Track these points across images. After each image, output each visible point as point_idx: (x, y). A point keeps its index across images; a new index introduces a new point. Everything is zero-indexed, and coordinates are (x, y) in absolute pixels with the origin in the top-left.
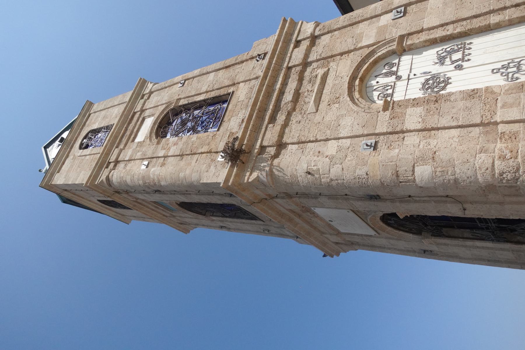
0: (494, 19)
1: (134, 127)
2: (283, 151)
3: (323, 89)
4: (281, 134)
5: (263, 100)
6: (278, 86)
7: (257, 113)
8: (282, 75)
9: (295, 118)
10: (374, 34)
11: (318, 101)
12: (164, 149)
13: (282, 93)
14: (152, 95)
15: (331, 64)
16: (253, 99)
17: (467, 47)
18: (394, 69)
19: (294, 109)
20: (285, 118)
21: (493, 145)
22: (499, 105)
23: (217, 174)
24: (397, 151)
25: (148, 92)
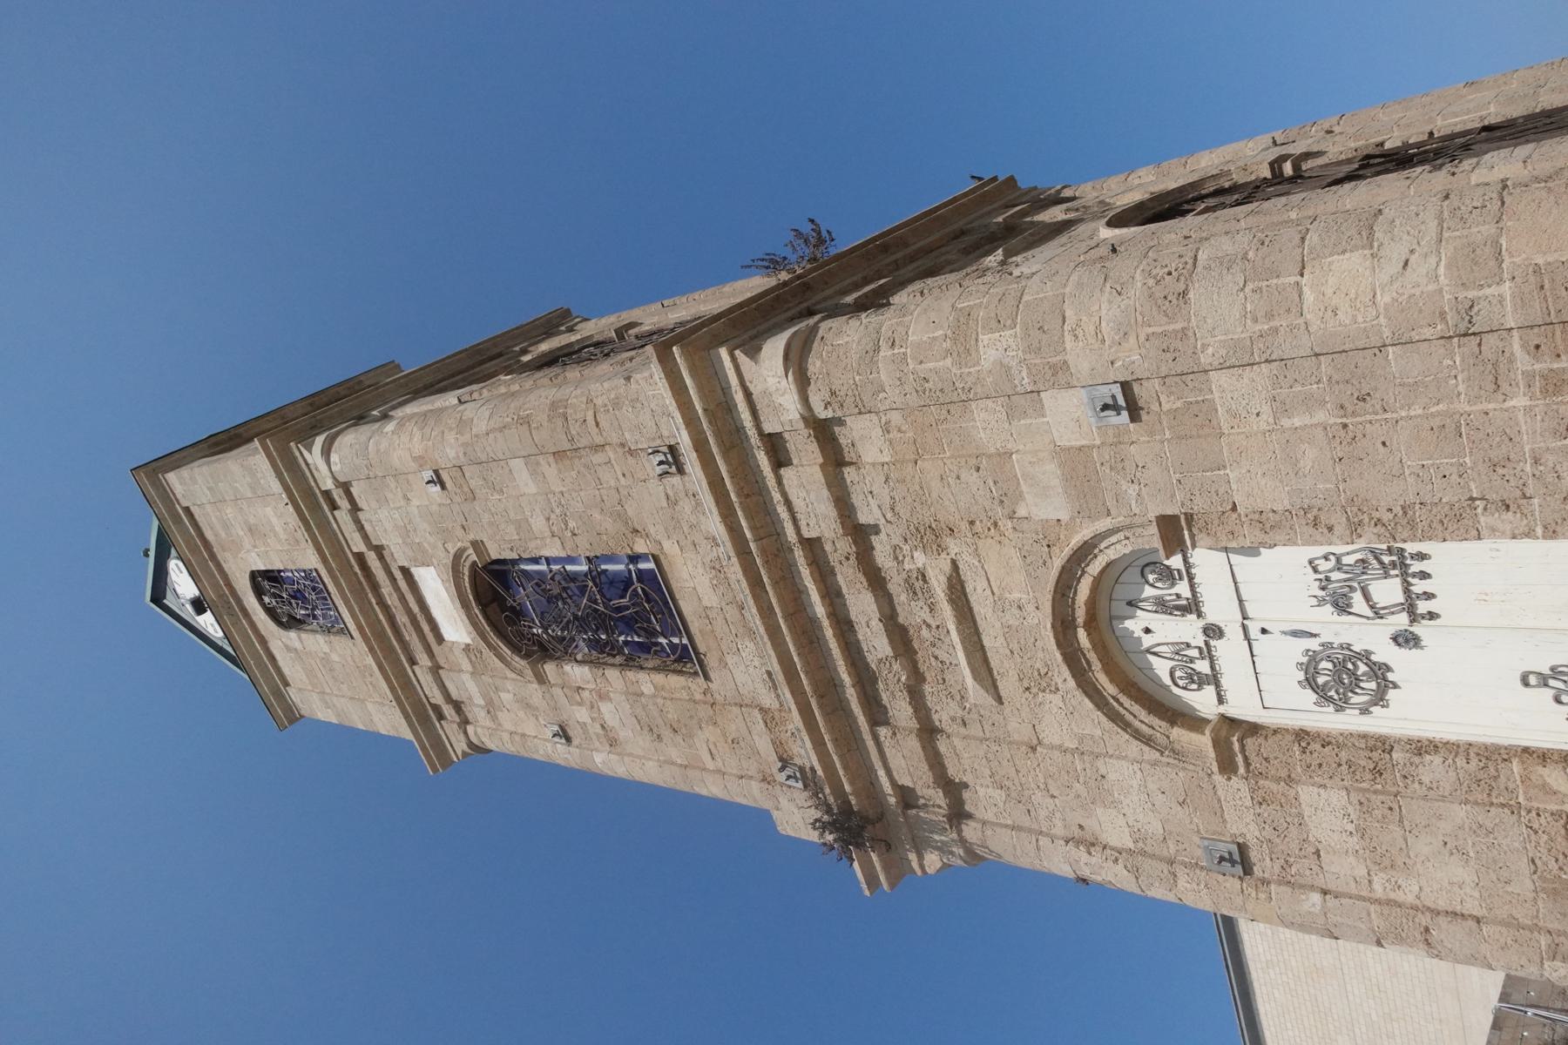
1: (402, 598)
3: (978, 633)
5: (806, 663)
6: (820, 610)
7: (821, 707)
8: (805, 572)
10: (1056, 482)
11: (983, 671)
13: (844, 626)
15: (954, 546)
16: (751, 602)
17: (1416, 567)
18: (1183, 588)
20: (910, 710)
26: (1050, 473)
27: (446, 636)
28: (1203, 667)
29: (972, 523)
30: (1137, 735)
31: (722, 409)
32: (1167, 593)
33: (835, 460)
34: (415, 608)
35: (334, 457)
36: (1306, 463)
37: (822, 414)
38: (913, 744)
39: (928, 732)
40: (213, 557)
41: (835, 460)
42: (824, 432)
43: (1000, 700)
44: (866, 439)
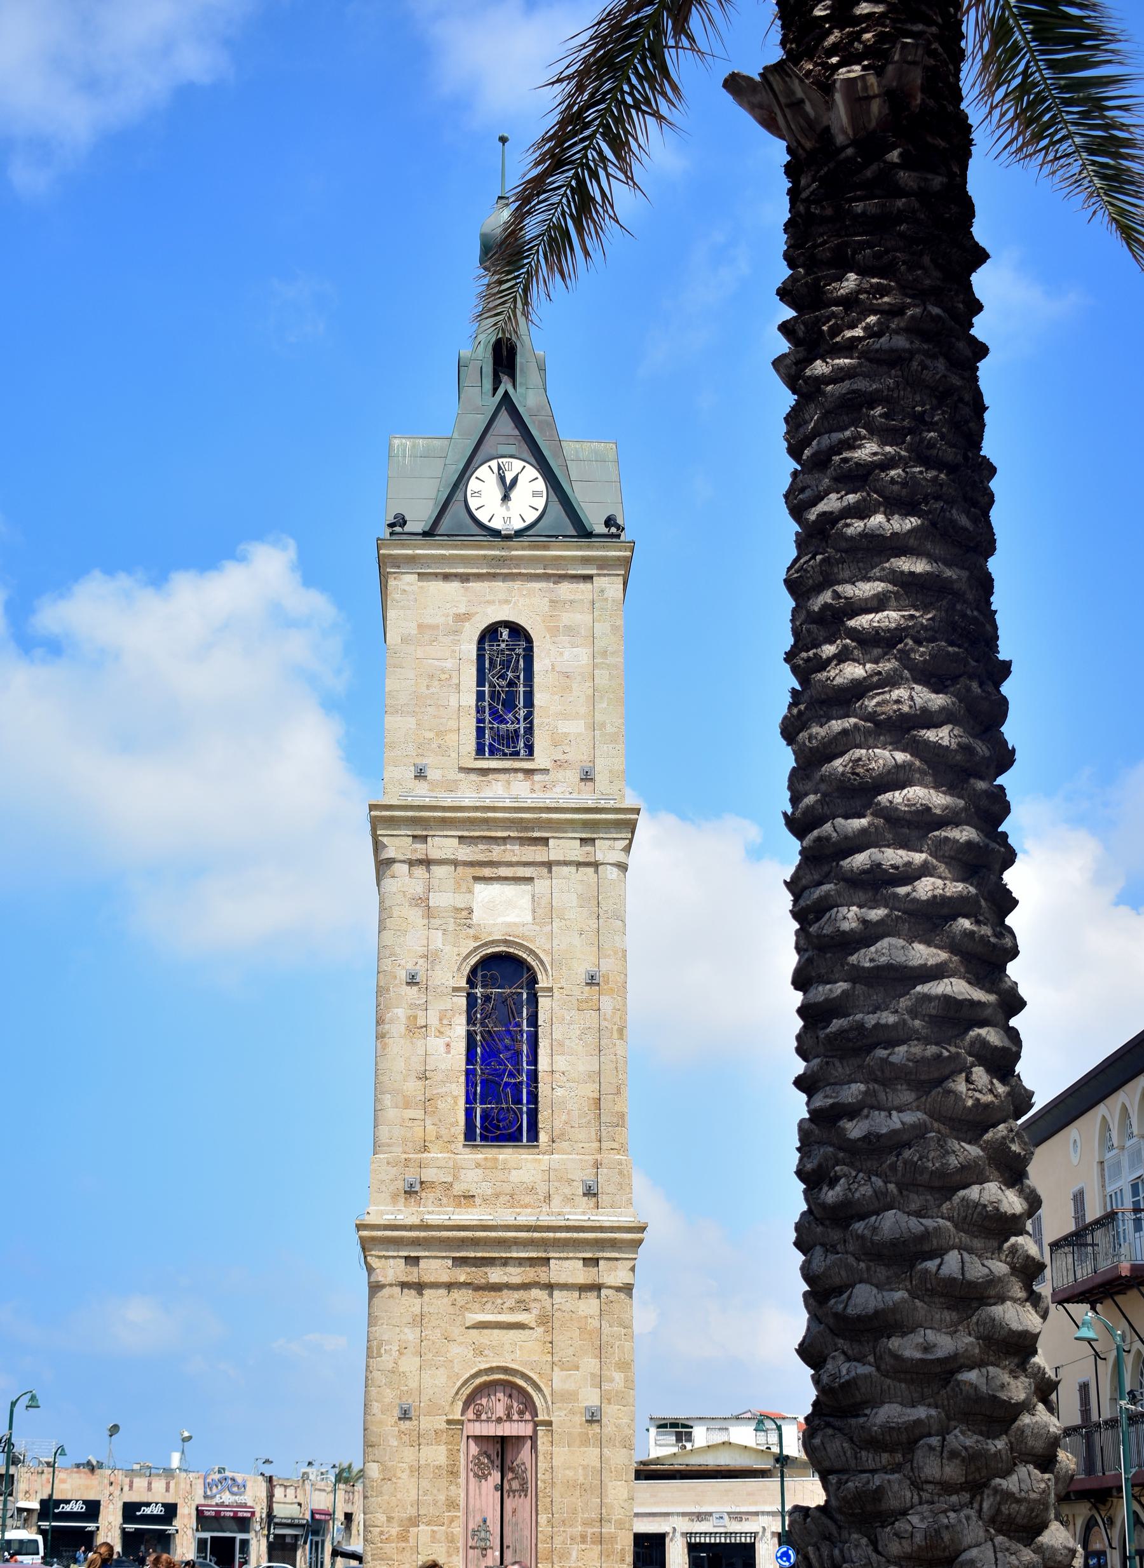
0: (543, 1519)
1: (510, 864)
2: (413, 1292)
4: (435, 1285)
9: (461, 1296)
12: (441, 1020)
13: (505, 1262)
14: (590, 870)
15: (540, 1330)
18: (516, 1417)
19: (478, 1288)
21: (395, 1525)
22: (435, 1528)
23: (384, 1188)
24: (396, 1444)
25: (599, 857)
26: (570, 1386)
27: (479, 887)
28: (484, 1417)
29: (551, 1343)
30: (459, 1389)
31: (613, 1244)
32: (515, 1410)
33: (583, 1288)
34: (504, 872)
35: (615, 870)
36: (567, 1472)
37: (604, 1292)
38: (445, 1278)
39: (449, 1286)
40: (546, 577)
41: (583, 1288)
42: (596, 1288)
43: (467, 1328)
44: (589, 1305)
